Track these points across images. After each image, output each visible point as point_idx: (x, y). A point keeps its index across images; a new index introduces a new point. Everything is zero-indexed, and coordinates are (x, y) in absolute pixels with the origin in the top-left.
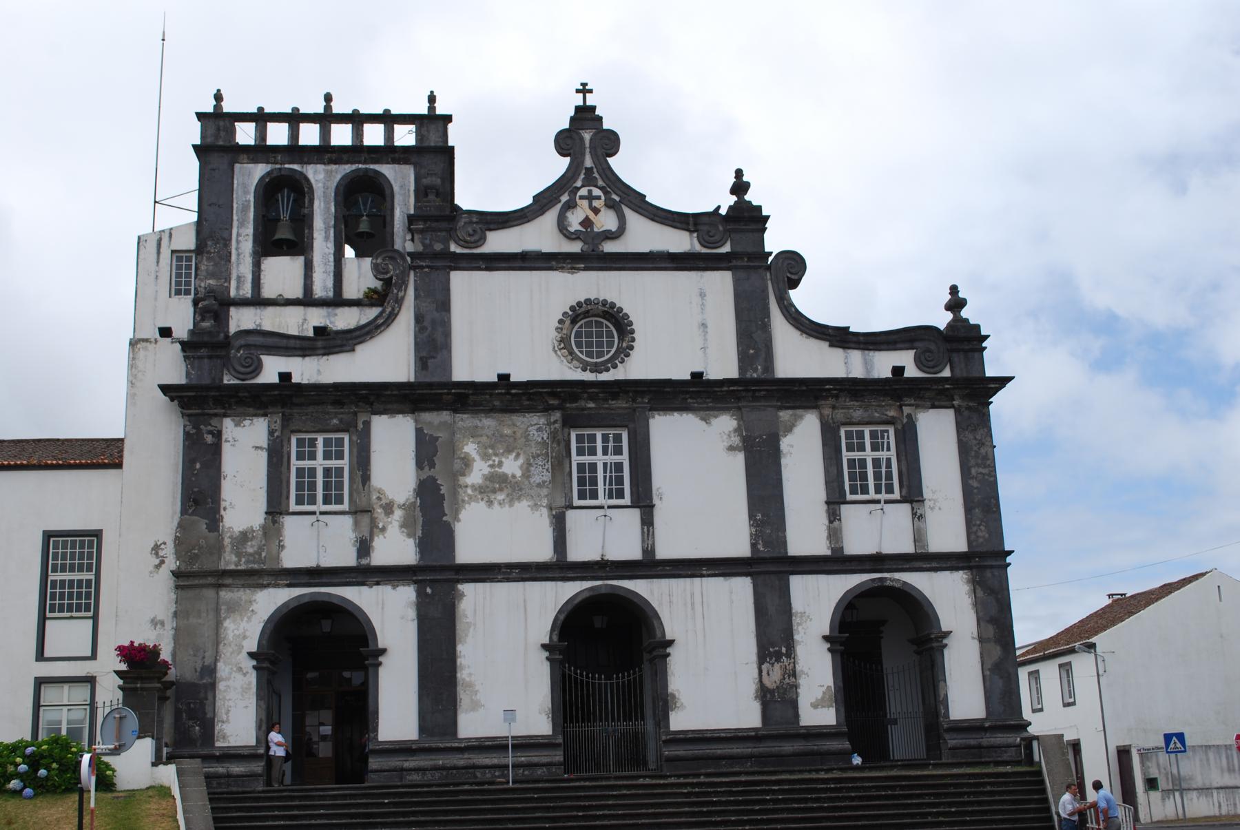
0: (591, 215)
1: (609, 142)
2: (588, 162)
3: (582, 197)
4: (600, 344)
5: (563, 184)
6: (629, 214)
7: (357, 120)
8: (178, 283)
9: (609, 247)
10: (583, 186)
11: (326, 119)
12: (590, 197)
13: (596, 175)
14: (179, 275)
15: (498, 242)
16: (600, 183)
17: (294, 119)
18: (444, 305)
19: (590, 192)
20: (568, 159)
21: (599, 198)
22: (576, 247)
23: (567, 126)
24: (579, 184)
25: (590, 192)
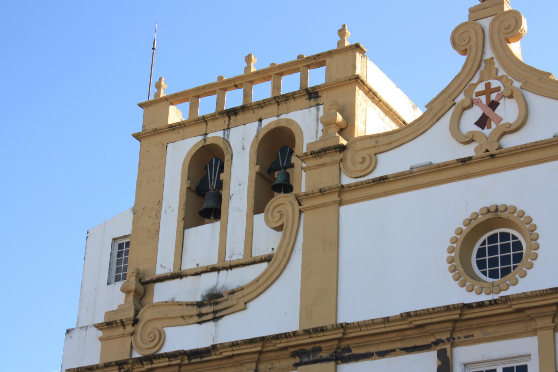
0: (489, 112)
1: (510, 26)
2: (489, 54)
3: (478, 94)
4: (505, 260)
5: (461, 83)
6: (534, 99)
7: (276, 73)
8: (118, 270)
9: (511, 142)
10: (480, 81)
11: (245, 81)
12: (489, 91)
13: (497, 65)
14: (119, 262)
15: (390, 164)
16: (502, 72)
17: (221, 87)
18: (332, 245)
19: (488, 85)
20: (465, 57)
21: (498, 89)
22: (469, 151)
23: (466, 19)
24: (475, 80)
25: (488, 85)
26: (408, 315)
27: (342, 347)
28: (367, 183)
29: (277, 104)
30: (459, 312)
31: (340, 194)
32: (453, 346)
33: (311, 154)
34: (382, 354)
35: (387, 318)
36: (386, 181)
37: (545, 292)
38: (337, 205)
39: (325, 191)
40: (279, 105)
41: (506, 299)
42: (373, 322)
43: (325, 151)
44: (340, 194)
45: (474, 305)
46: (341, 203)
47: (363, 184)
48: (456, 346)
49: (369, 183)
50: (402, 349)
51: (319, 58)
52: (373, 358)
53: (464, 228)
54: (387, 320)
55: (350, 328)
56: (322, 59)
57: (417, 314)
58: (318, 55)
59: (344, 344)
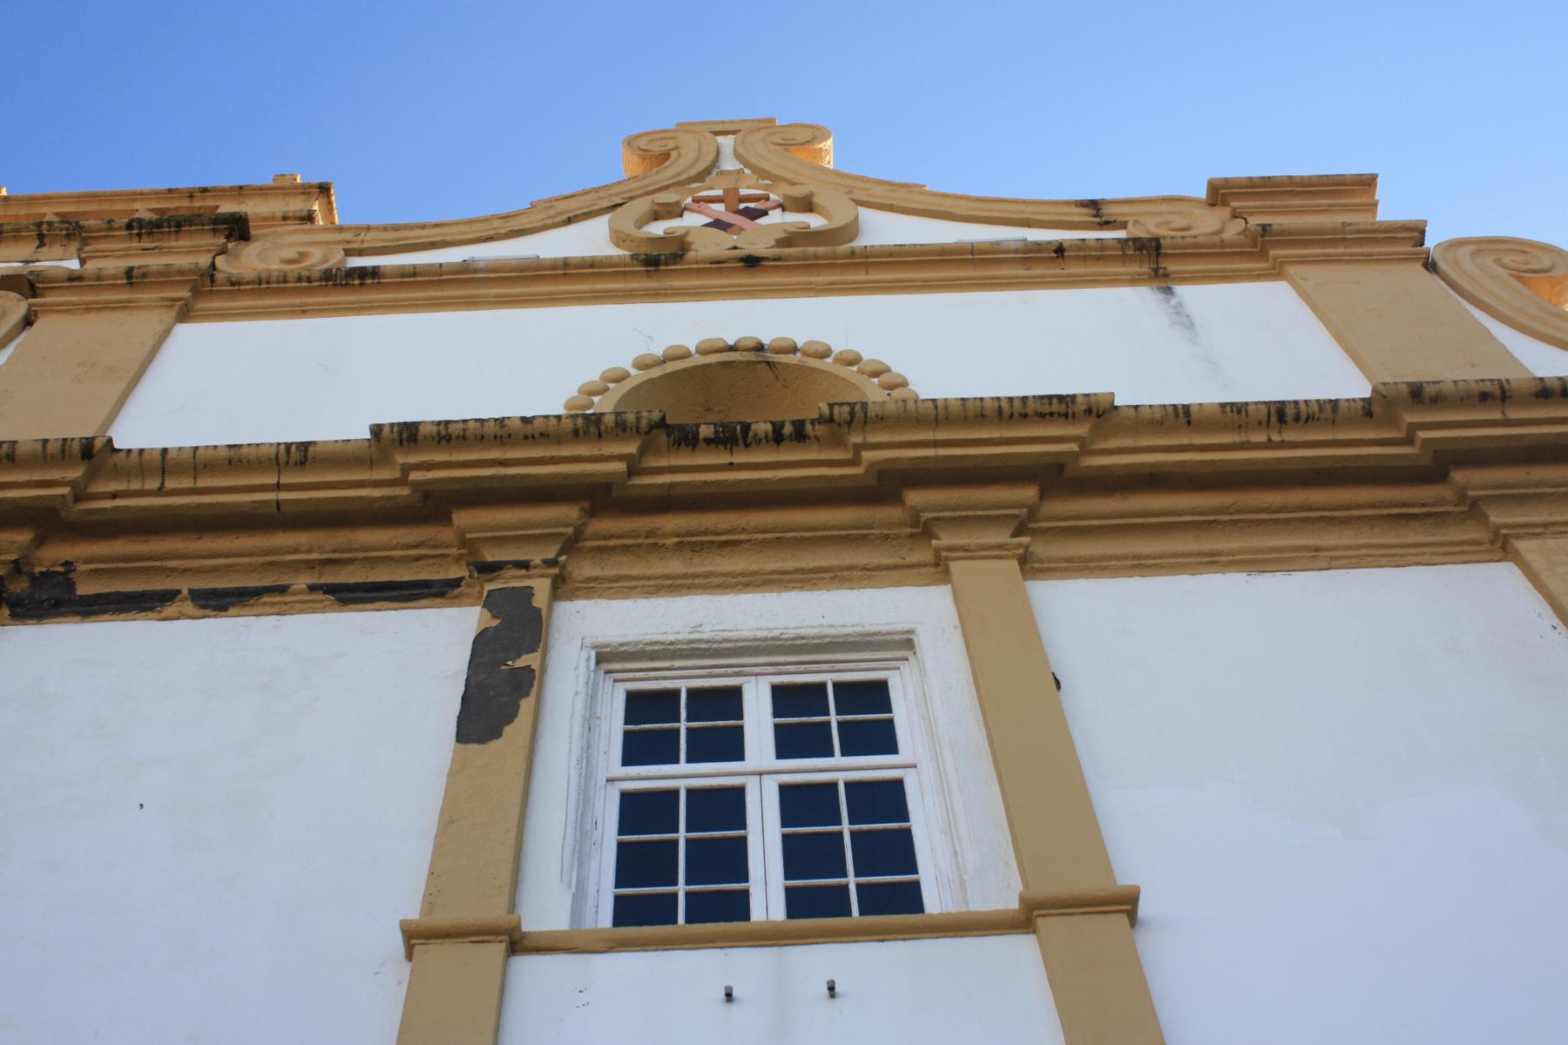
26: (408, 434)
27: (37, 570)
28: (300, 279)
29: (37, 243)
30: (631, 448)
31: (197, 293)
32: (562, 588)
33: (129, 226)
34: (216, 602)
35: (305, 446)
36: (369, 281)
37: (1017, 404)
38: (174, 313)
39: (144, 276)
40: (42, 245)
41: (852, 413)
42: (236, 459)
43: (179, 225)
44: (197, 293)
45: (706, 431)
46: (186, 314)
47: (285, 281)
48: (572, 596)
49: (309, 280)
50: (313, 588)
51: (204, 198)
52: (169, 610)
53: (633, 372)
54: (300, 455)
55: (117, 472)
56: (211, 203)
57: (447, 435)
58: (204, 190)
59: (53, 555)
